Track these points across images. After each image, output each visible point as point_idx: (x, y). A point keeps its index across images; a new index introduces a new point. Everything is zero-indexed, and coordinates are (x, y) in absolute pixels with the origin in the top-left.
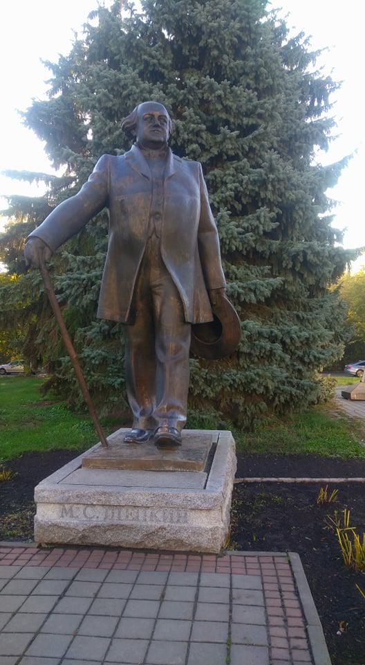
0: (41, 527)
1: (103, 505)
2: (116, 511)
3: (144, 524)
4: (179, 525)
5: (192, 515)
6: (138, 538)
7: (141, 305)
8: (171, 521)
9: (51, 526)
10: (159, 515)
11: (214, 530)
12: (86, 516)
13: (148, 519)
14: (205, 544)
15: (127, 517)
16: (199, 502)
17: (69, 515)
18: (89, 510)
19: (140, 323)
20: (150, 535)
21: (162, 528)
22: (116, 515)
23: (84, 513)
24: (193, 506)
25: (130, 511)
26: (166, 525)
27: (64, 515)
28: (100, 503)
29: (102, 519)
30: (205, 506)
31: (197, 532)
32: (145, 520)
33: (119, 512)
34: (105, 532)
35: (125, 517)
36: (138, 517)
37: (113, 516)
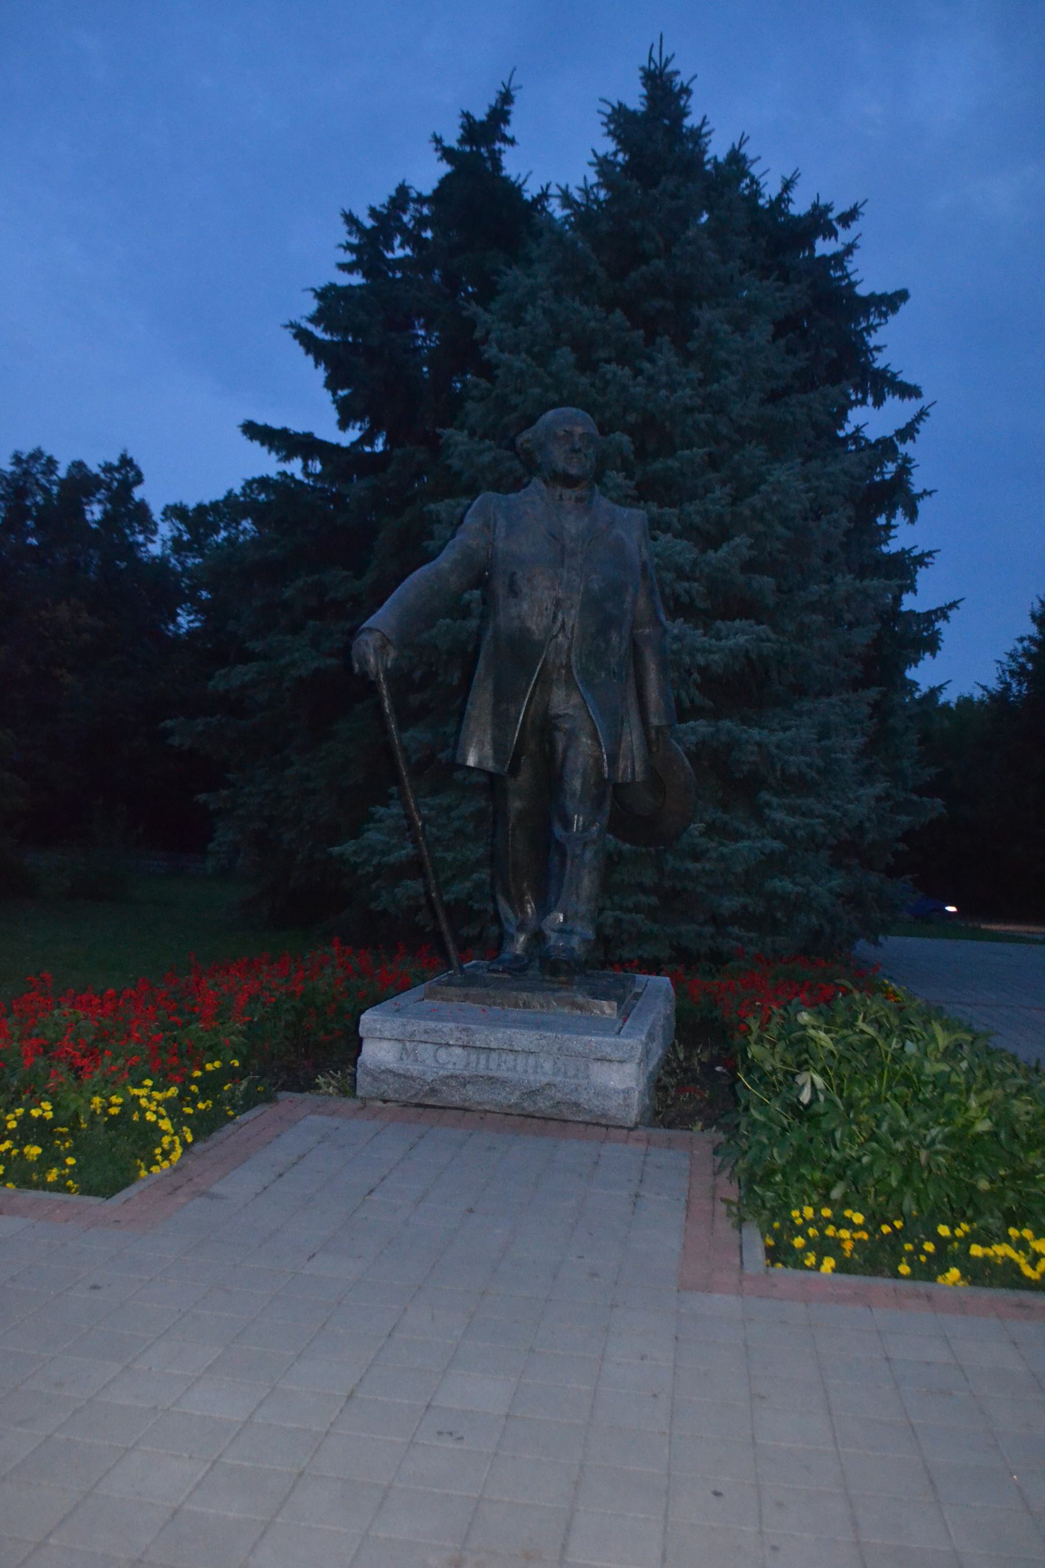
0: (368, 1072)
1: (464, 1047)
4: (576, 1081)
5: (596, 1068)
6: (513, 1099)
7: (532, 745)
8: (565, 1075)
9: (383, 1071)
10: (548, 1066)
11: (627, 1092)
12: (437, 1061)
13: (530, 1071)
14: (613, 1112)
15: (499, 1065)
16: (609, 1050)
18: (443, 1054)
19: (524, 778)
20: (532, 1093)
22: (483, 1062)
23: (435, 1056)
24: (599, 1056)
25: (504, 1056)
26: (558, 1079)
27: (404, 1057)
28: (461, 1043)
29: (461, 1067)
30: (616, 1056)
31: (603, 1093)
33: (488, 1058)
34: (465, 1085)
36: (515, 1067)
37: (478, 1063)
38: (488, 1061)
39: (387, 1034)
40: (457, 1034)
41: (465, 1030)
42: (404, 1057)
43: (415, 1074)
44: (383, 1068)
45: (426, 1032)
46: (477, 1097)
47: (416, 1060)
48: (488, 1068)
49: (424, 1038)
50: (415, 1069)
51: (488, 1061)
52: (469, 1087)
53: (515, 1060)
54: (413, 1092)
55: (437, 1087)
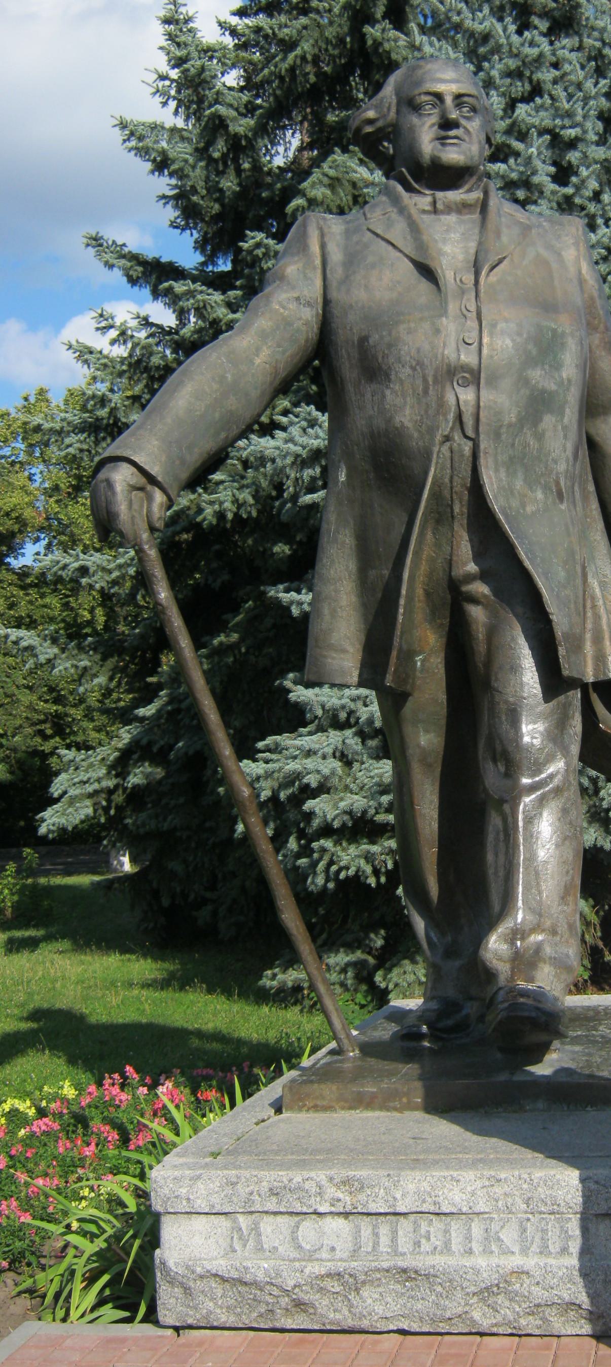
1: (346, 1215)
2: (384, 1230)
3: (468, 1262)
9: (202, 1277)
10: (509, 1236)
13: (475, 1246)
15: (418, 1244)
17: (251, 1244)
18: (308, 1230)
21: (521, 1273)
22: (384, 1240)
23: (294, 1239)
26: (531, 1262)
27: (237, 1246)
29: (345, 1255)
32: (470, 1252)
33: (394, 1233)
34: (357, 1290)
35: (404, 1245)
36: (447, 1244)
37: (376, 1244)
38: (394, 1239)
39: (201, 1204)
40: (331, 1192)
41: (346, 1182)
42: (237, 1246)
43: (261, 1276)
44: (199, 1270)
45: (273, 1192)
46: (379, 1309)
47: (260, 1248)
48: (396, 1253)
49: (271, 1206)
50: (260, 1268)
51: (394, 1239)
52: (365, 1292)
53: (446, 1231)
54: (263, 1309)
55: (306, 1298)
